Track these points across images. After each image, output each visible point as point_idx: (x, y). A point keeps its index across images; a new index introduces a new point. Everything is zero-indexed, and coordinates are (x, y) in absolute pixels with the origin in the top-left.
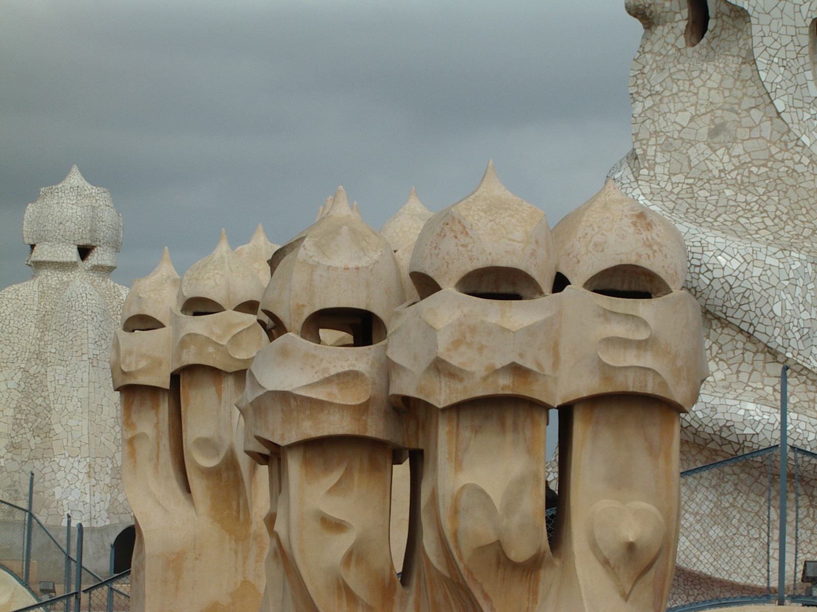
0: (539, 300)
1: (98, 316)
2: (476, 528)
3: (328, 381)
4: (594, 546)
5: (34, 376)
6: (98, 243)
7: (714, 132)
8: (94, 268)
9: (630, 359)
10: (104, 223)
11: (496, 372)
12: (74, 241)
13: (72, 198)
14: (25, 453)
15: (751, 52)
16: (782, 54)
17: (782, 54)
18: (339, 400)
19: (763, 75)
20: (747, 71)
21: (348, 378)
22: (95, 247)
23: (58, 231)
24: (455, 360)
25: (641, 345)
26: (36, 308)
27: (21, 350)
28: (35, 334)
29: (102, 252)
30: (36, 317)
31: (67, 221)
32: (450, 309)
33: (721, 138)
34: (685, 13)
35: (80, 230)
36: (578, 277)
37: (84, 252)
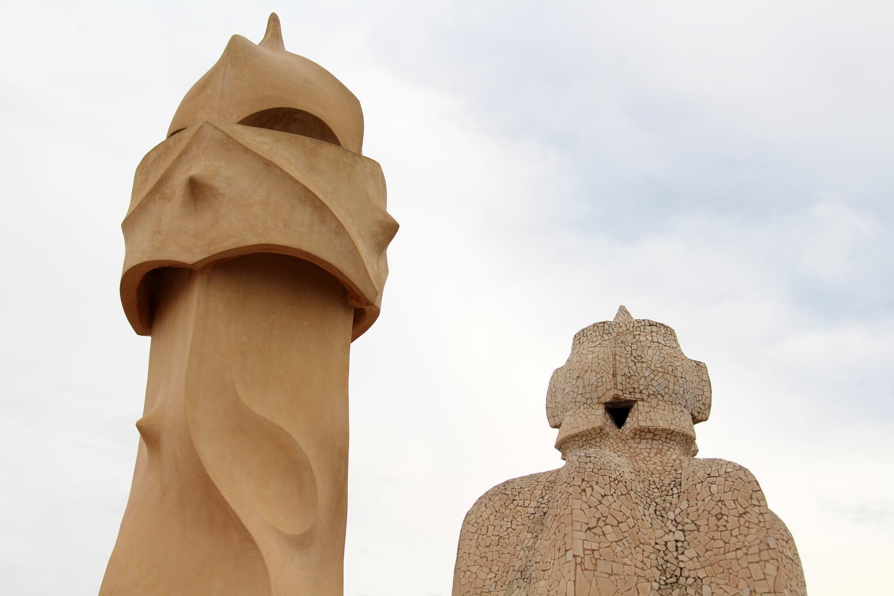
1: (596, 487)
6: (638, 396)
8: (635, 434)
10: (644, 365)
12: (598, 398)
13: (594, 339)
22: (635, 401)
23: (576, 390)
26: (534, 504)
27: (501, 569)
28: (526, 542)
29: (647, 409)
30: (532, 517)
31: (586, 371)
35: (604, 379)
37: (618, 412)
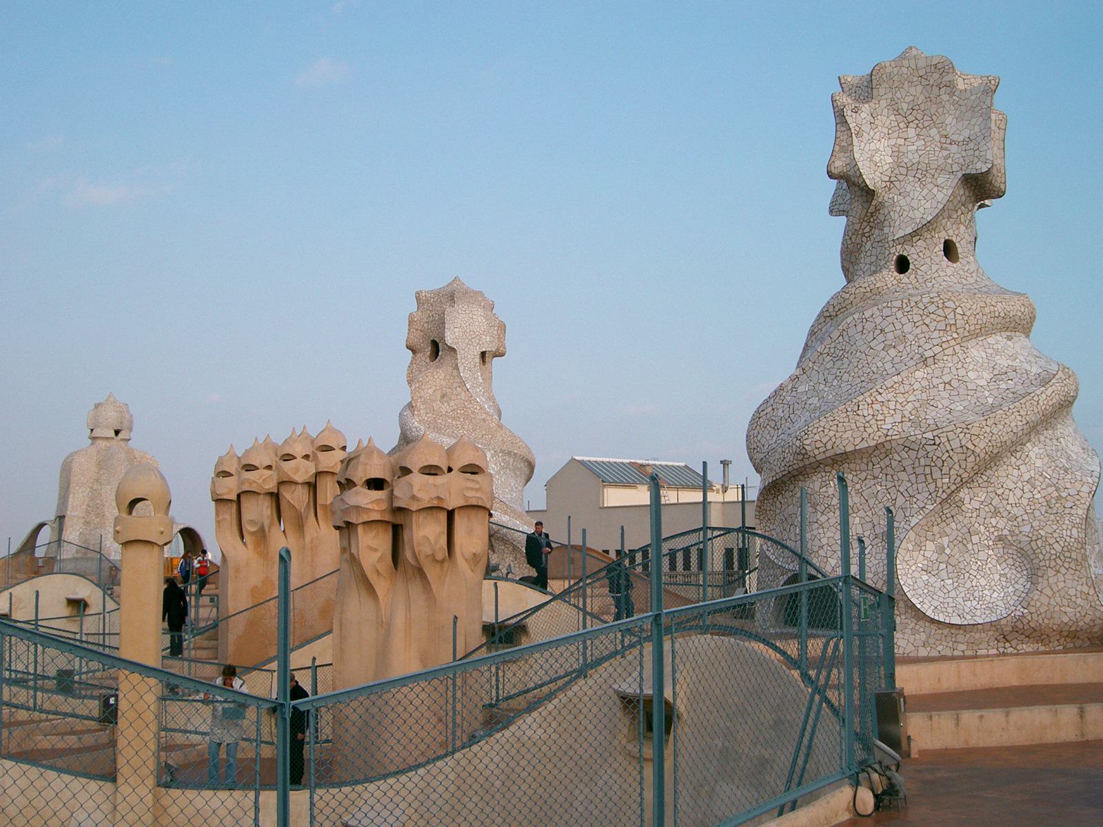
0: (445, 476)
2: (426, 549)
3: (373, 502)
4: (463, 554)
5: (95, 490)
7: (443, 396)
9: (473, 494)
11: (432, 499)
14: (92, 526)
15: (457, 365)
16: (469, 366)
17: (469, 366)
18: (376, 508)
19: (462, 374)
20: (455, 372)
21: (378, 501)
24: (419, 495)
25: (477, 490)
32: (417, 479)
33: (445, 399)
34: (430, 348)
36: (456, 467)
37: (117, 432)
